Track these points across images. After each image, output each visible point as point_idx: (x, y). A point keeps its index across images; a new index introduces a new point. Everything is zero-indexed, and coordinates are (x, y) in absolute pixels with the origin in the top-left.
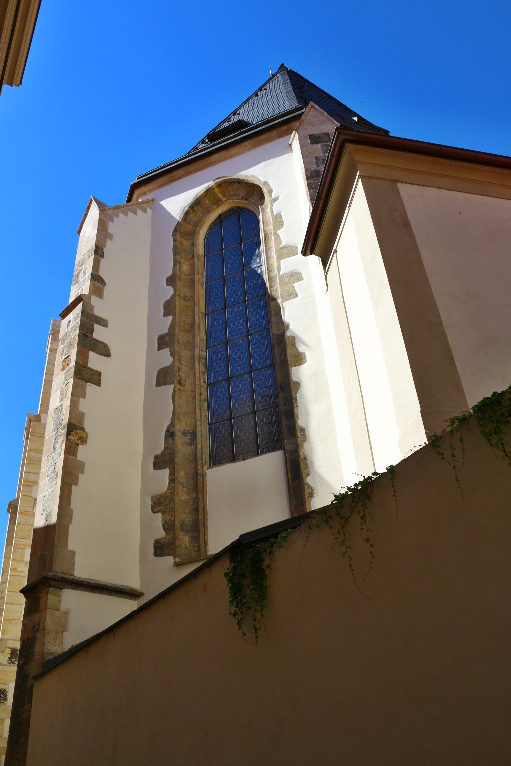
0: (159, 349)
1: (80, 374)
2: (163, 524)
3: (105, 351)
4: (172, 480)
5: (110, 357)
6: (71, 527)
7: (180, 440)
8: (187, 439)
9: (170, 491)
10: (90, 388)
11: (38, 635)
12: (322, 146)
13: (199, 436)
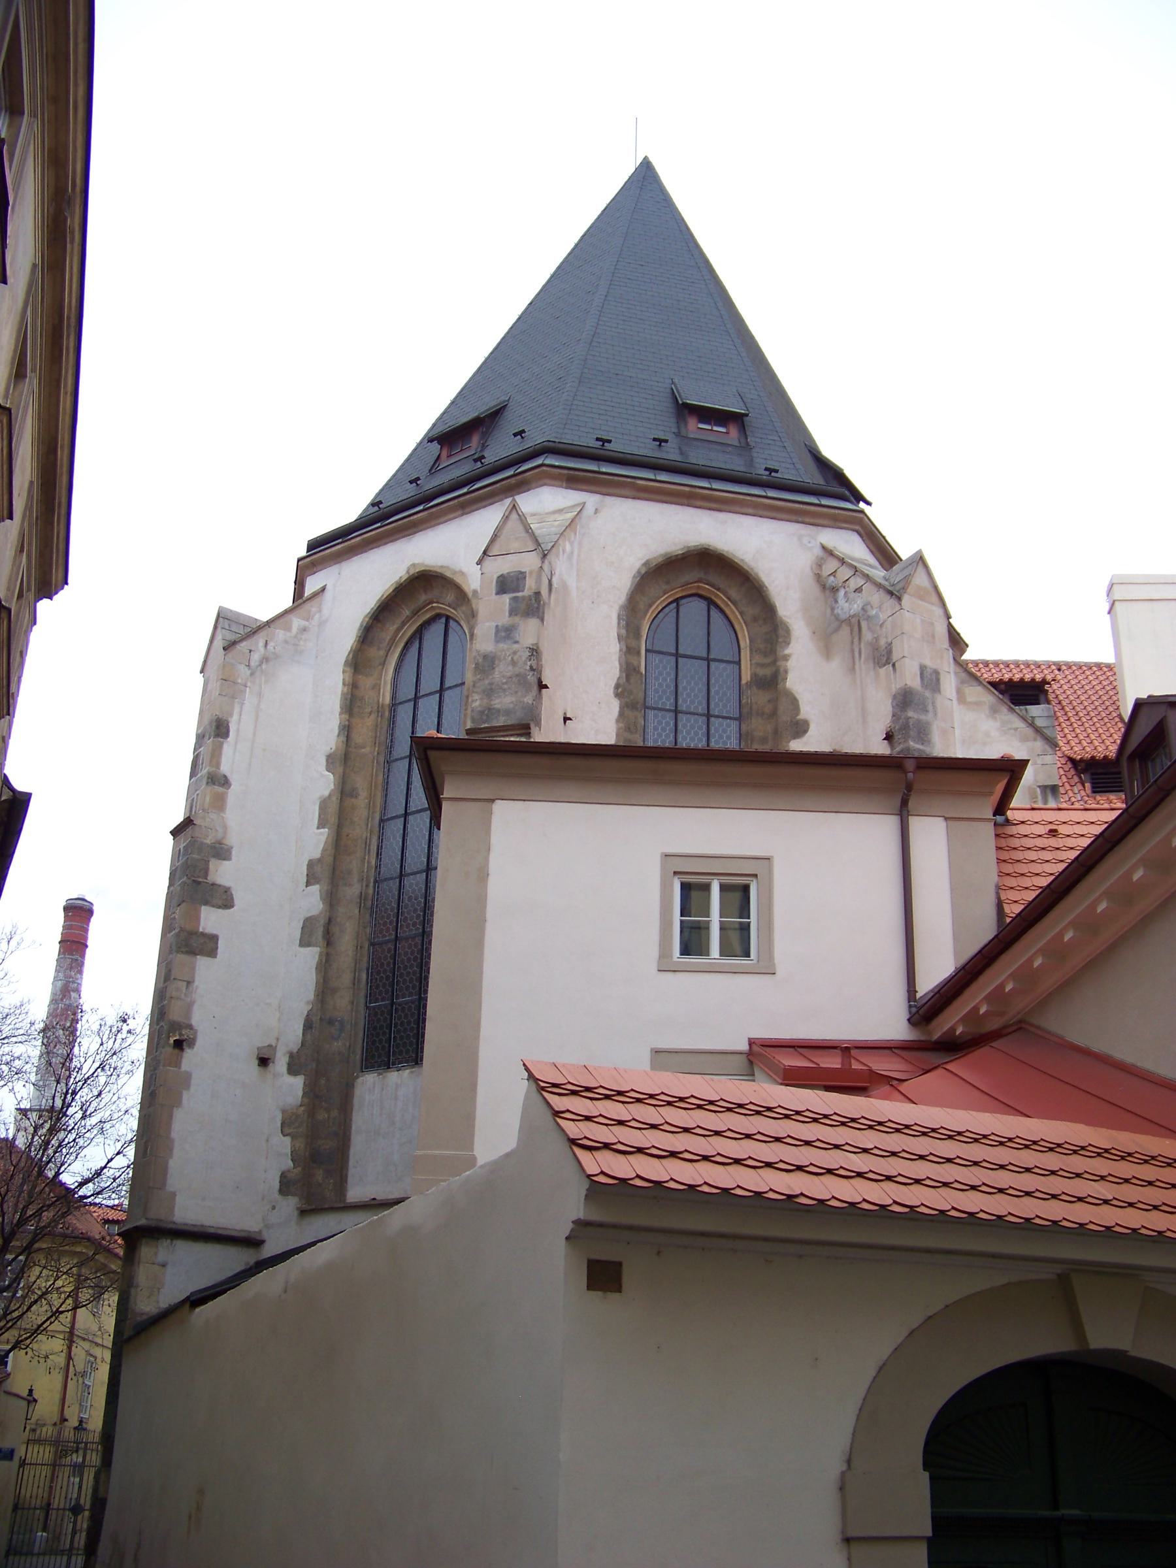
0: (308, 884)
2: (292, 1152)
3: (226, 899)
6: (171, 1163)
9: (303, 1108)
10: (202, 962)
11: (133, 1291)
12: (510, 599)
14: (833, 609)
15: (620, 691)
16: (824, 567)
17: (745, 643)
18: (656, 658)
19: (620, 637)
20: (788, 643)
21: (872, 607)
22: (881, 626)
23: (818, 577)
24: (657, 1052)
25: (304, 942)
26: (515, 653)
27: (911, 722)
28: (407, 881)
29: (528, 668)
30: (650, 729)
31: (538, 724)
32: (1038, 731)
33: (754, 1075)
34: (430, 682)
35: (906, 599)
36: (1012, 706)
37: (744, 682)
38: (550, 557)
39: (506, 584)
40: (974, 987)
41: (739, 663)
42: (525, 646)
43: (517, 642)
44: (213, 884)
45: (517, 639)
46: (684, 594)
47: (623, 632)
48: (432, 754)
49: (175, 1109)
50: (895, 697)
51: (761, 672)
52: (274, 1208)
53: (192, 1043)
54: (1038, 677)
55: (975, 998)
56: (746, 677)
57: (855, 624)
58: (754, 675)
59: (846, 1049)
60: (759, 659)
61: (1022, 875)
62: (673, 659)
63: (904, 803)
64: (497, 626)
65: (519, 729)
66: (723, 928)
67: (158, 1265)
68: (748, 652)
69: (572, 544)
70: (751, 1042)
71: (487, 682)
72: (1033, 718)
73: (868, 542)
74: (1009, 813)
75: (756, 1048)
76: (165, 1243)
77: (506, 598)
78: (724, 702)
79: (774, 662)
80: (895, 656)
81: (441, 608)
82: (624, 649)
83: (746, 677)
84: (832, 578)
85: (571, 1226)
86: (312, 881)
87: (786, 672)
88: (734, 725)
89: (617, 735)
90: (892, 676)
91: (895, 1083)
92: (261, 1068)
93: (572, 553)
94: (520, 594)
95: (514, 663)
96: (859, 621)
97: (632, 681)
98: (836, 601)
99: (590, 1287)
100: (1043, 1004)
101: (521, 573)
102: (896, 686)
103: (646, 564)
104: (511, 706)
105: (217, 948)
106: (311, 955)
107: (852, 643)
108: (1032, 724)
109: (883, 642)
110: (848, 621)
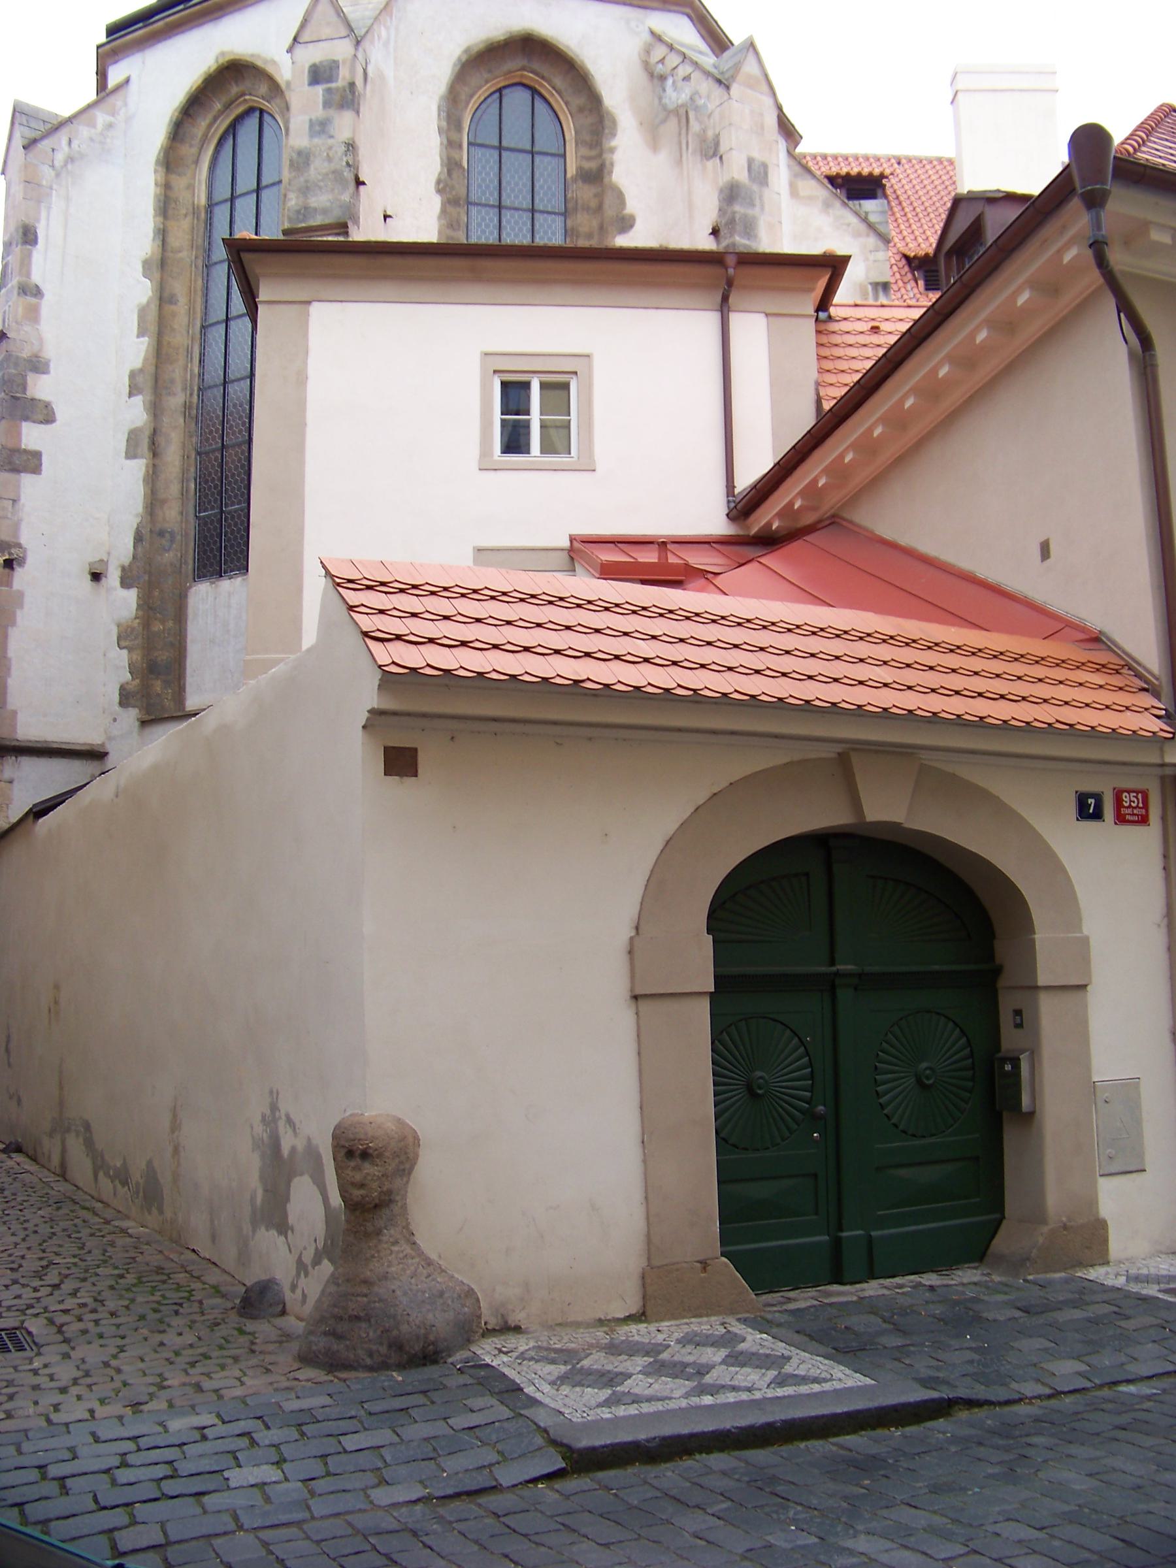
0: (131, 395)
3: (47, 414)
5: (54, 425)
6: (10, 682)
9: (137, 621)
10: (27, 479)
12: (324, 90)
14: (660, 99)
15: (442, 187)
16: (652, 53)
17: (570, 134)
18: (478, 152)
19: (440, 130)
20: (614, 135)
21: (700, 97)
22: (709, 116)
23: (646, 65)
24: (479, 550)
25: (131, 454)
26: (330, 148)
27: (737, 217)
28: (231, 389)
29: (344, 163)
30: (473, 225)
31: (356, 222)
32: (871, 226)
33: (575, 571)
34: (247, 182)
35: (735, 89)
36: (846, 201)
37: (569, 175)
38: (366, 44)
39: (319, 75)
40: (789, 482)
41: (564, 156)
42: (341, 140)
43: (332, 137)
44: (32, 399)
45: (332, 133)
46: (507, 83)
47: (444, 124)
48: (246, 257)
49: (10, 628)
50: (721, 191)
51: (587, 165)
52: (115, 720)
53: (22, 561)
54: (877, 172)
55: (790, 494)
56: (572, 171)
57: (683, 115)
58: (580, 169)
59: (662, 545)
60: (584, 151)
61: (843, 371)
62: (496, 153)
63: (725, 299)
64: (311, 120)
65: (335, 228)
66: (544, 426)
68: (574, 145)
69: (387, 29)
70: (572, 539)
71: (302, 179)
72: (867, 213)
73: (699, 26)
74: (832, 310)
75: (576, 545)
77: (319, 89)
78: (549, 196)
79: (600, 155)
80: (723, 148)
81: (254, 101)
82: (445, 142)
83: (572, 171)
84: (660, 66)
85: (367, 714)
86: (135, 392)
87: (612, 164)
88: (559, 220)
89: (440, 233)
90: (719, 170)
91: (710, 576)
92: (94, 584)
93: (388, 39)
94: (333, 85)
95: (329, 159)
96: (687, 112)
97: (455, 175)
98: (664, 90)
99: (387, 772)
100: (855, 499)
101: (334, 61)
102: (723, 179)
103: (467, 51)
104: (328, 204)
106: (138, 467)
107: (680, 134)
108: (865, 220)
109: (710, 134)
110: (676, 112)
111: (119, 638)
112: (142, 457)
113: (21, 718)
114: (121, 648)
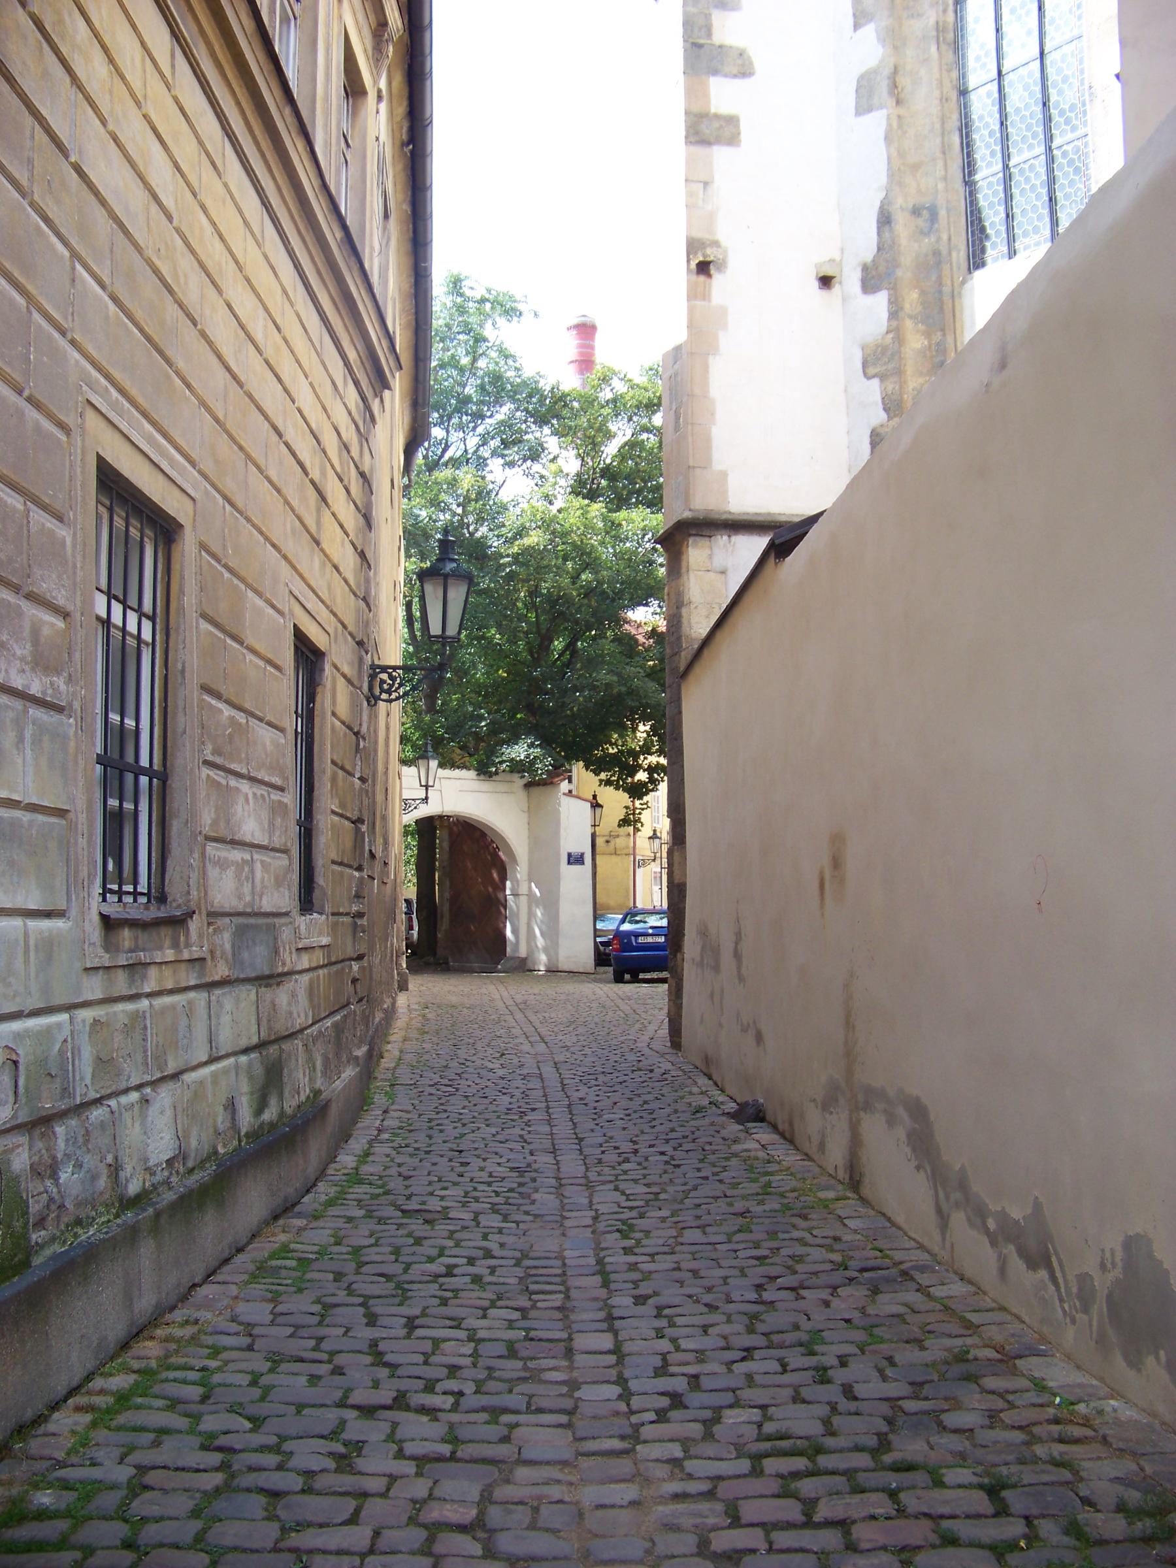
1: (697, 133)
3: (743, 65)
4: (895, 313)
5: (753, 78)
7: (903, 226)
8: (921, 222)
9: (891, 336)
10: (720, 153)
11: (684, 611)
13: (942, 213)
25: (863, 107)
44: (721, 47)
49: (711, 359)
53: (722, 266)
67: (716, 572)
76: (722, 540)
92: (824, 293)
105: (739, 134)
106: (877, 122)
111: (865, 365)
112: (881, 107)
113: (733, 483)
114: (867, 377)
